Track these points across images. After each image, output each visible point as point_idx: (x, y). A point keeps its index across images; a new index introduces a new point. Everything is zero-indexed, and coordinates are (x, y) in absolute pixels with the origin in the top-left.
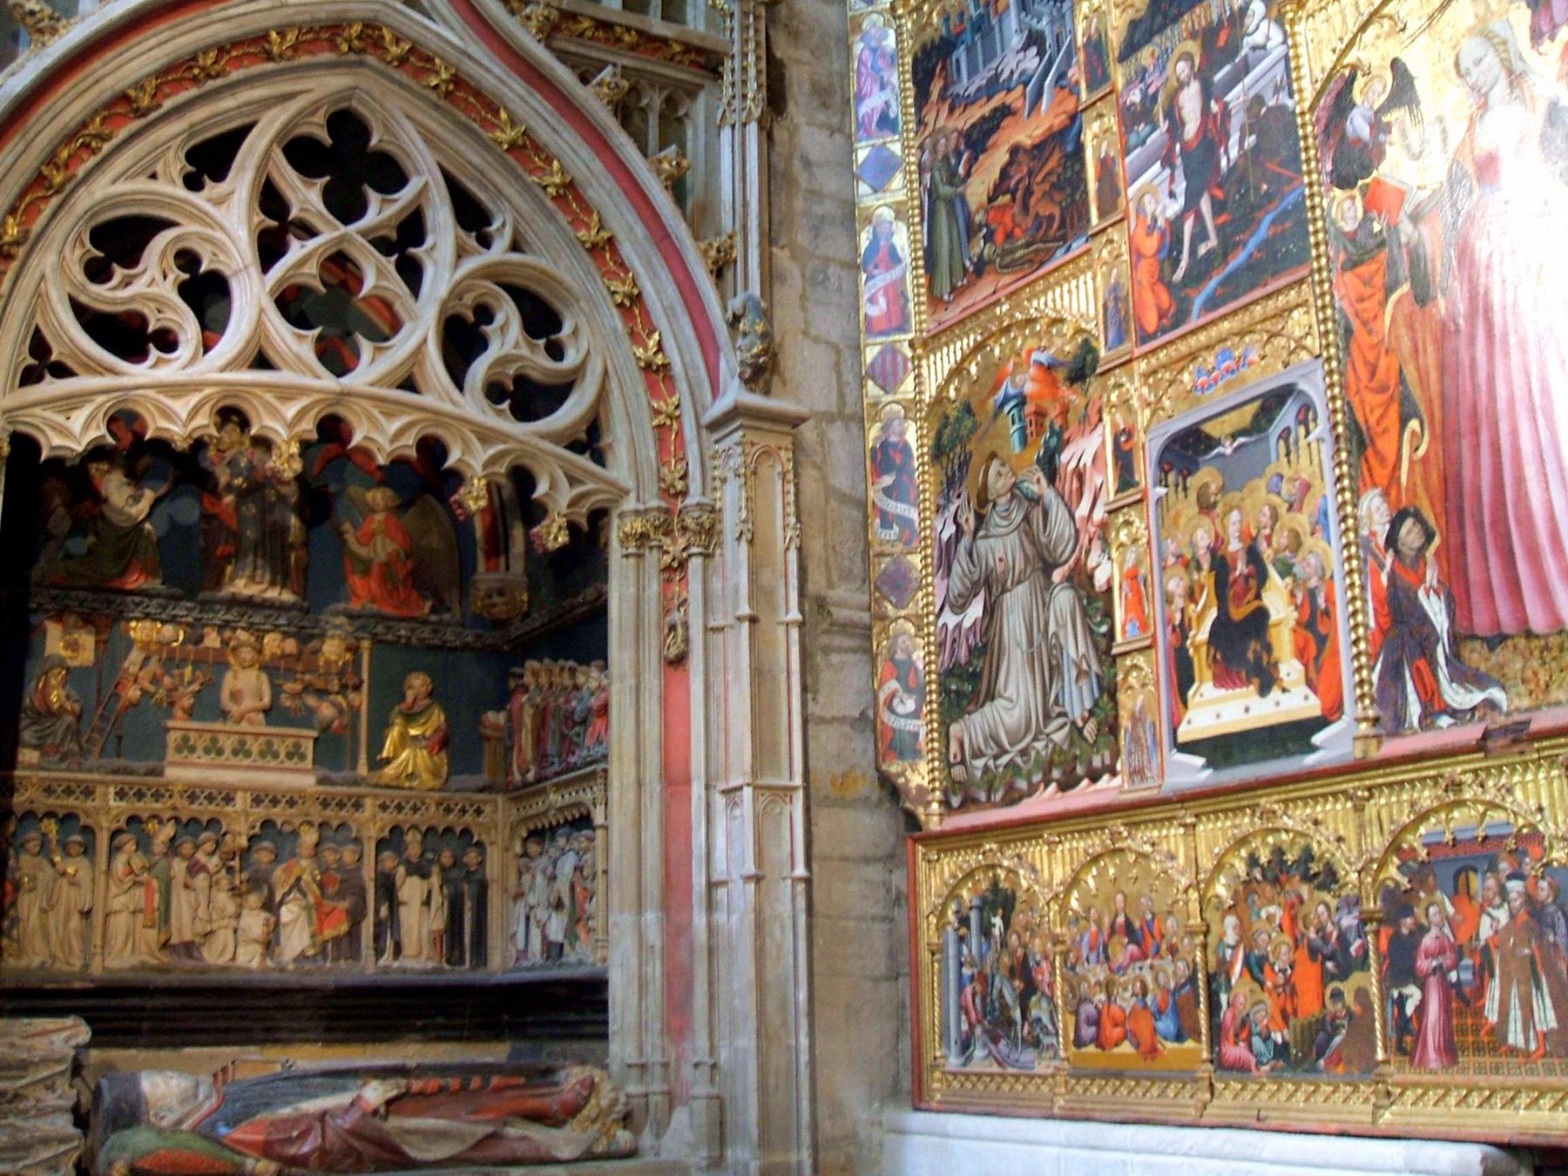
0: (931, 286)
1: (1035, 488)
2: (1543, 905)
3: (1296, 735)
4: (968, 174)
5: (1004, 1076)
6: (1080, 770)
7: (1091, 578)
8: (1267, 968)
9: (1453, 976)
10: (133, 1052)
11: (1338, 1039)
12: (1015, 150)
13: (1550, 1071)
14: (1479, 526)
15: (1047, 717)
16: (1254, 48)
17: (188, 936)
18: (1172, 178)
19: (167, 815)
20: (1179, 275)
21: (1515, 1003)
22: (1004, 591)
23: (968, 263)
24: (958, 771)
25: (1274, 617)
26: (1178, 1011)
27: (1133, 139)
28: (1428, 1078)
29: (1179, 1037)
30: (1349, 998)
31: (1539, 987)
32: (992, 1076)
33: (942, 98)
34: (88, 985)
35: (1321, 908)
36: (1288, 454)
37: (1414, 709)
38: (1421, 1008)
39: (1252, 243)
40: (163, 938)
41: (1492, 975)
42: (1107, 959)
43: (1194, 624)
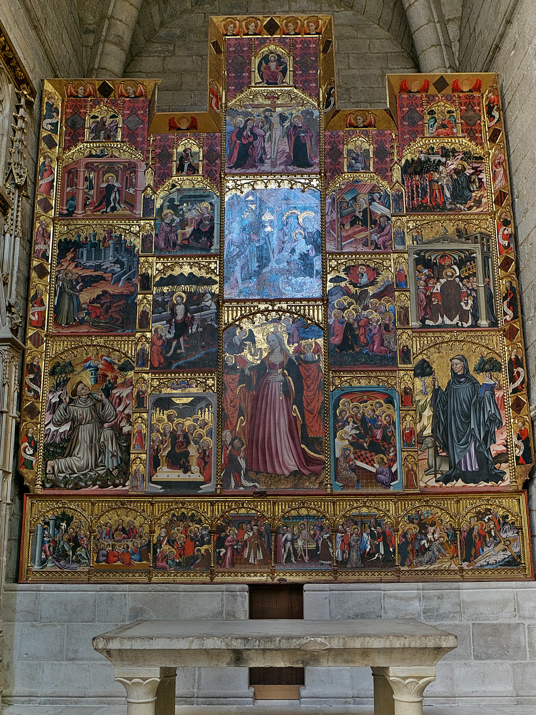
0: (55, 319)
1: (100, 397)
2: (262, 532)
3: (197, 485)
4: (81, 290)
5: (63, 572)
6: (109, 483)
7: (121, 429)
8: (175, 543)
9: (236, 547)
11: (198, 561)
12: (105, 292)
13: (260, 568)
14: (257, 446)
15: (97, 466)
16: (206, 306)
18: (170, 328)
20: (169, 355)
21: (252, 553)
22: (81, 424)
23: (76, 318)
24: (50, 476)
25: (191, 454)
26: (141, 553)
27: (156, 310)
28: (226, 570)
29: (140, 560)
30: (203, 551)
31: (259, 550)
32: (57, 572)
33: (73, 260)
35: (196, 529)
36: (201, 414)
37: (233, 484)
38: (225, 554)
39: (198, 356)
41: (247, 547)
42: (113, 538)
43: (162, 450)
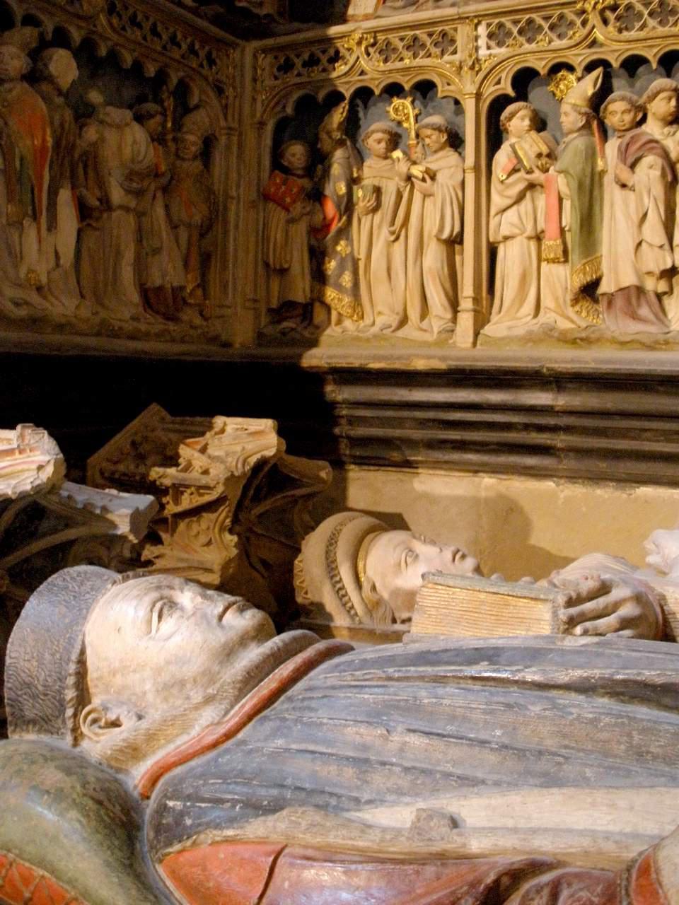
10: (549, 484)
17: (629, 279)
19: (579, 58)
34: (442, 366)
40: (579, 281)
